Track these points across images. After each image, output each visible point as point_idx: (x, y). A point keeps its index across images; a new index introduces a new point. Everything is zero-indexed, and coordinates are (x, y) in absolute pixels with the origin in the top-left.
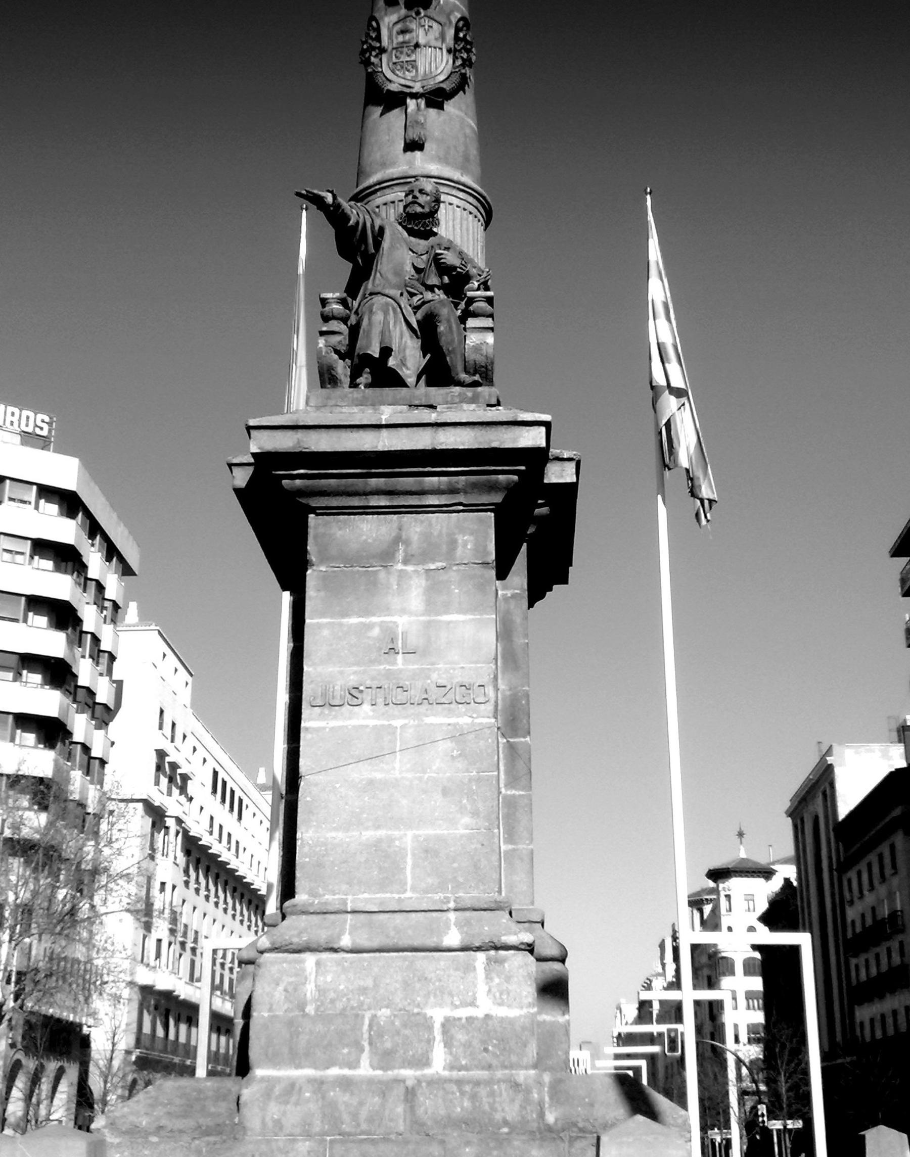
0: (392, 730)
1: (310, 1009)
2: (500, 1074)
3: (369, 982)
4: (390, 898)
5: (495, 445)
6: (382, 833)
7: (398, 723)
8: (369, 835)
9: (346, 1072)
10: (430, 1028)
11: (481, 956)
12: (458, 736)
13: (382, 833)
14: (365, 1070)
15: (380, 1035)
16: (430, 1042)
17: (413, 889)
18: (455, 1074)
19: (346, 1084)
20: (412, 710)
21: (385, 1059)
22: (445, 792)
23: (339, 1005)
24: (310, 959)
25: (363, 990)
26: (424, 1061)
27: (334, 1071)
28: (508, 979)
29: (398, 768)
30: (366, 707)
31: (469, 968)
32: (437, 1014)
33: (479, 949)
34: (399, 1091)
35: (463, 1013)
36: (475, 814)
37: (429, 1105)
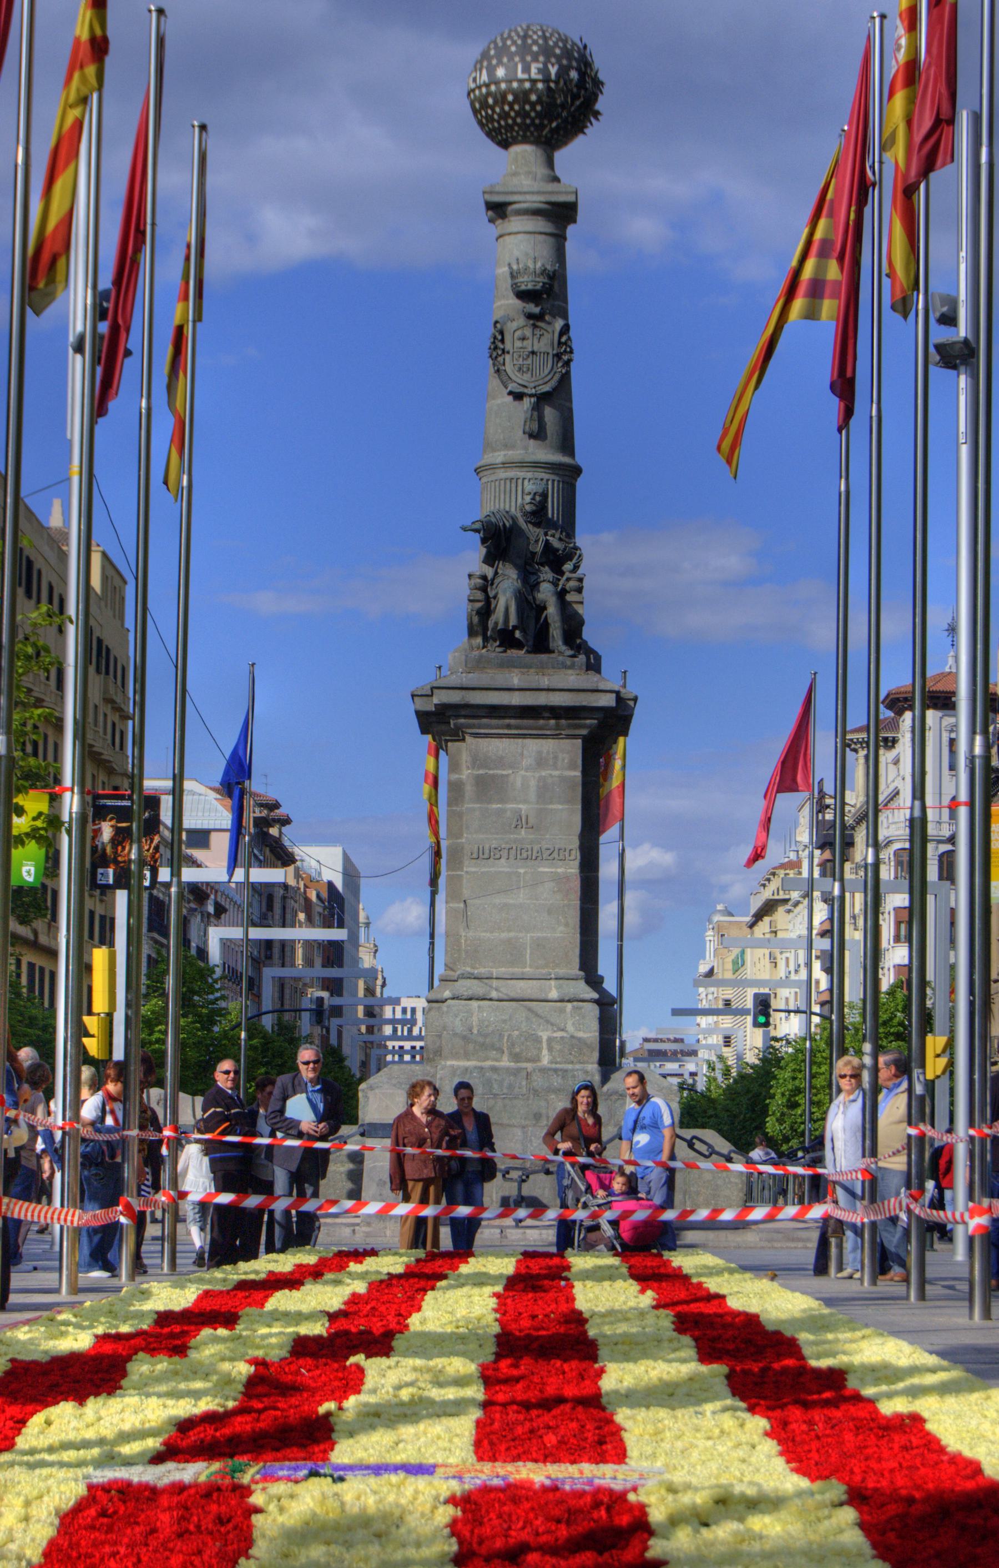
0: (518, 875)
1: (475, 1031)
2: (578, 1066)
3: (507, 1017)
4: (517, 970)
5: (584, 704)
6: (512, 934)
7: (522, 871)
8: (504, 935)
9: (497, 1064)
10: (541, 1042)
11: (569, 1005)
12: (557, 879)
13: (512, 934)
14: (505, 1062)
15: (513, 1045)
16: (540, 1049)
17: (531, 966)
18: (554, 1066)
19: (494, 1069)
20: (529, 863)
21: (516, 1057)
22: (549, 912)
23: (491, 1029)
24: (474, 1004)
25: (504, 1021)
26: (537, 1059)
27: (488, 1063)
28: (584, 1017)
29: (521, 897)
30: (503, 860)
31: (562, 1011)
32: (544, 1035)
33: (569, 1001)
34: (524, 1074)
35: (559, 1034)
36: (567, 925)
37: (539, 1081)
